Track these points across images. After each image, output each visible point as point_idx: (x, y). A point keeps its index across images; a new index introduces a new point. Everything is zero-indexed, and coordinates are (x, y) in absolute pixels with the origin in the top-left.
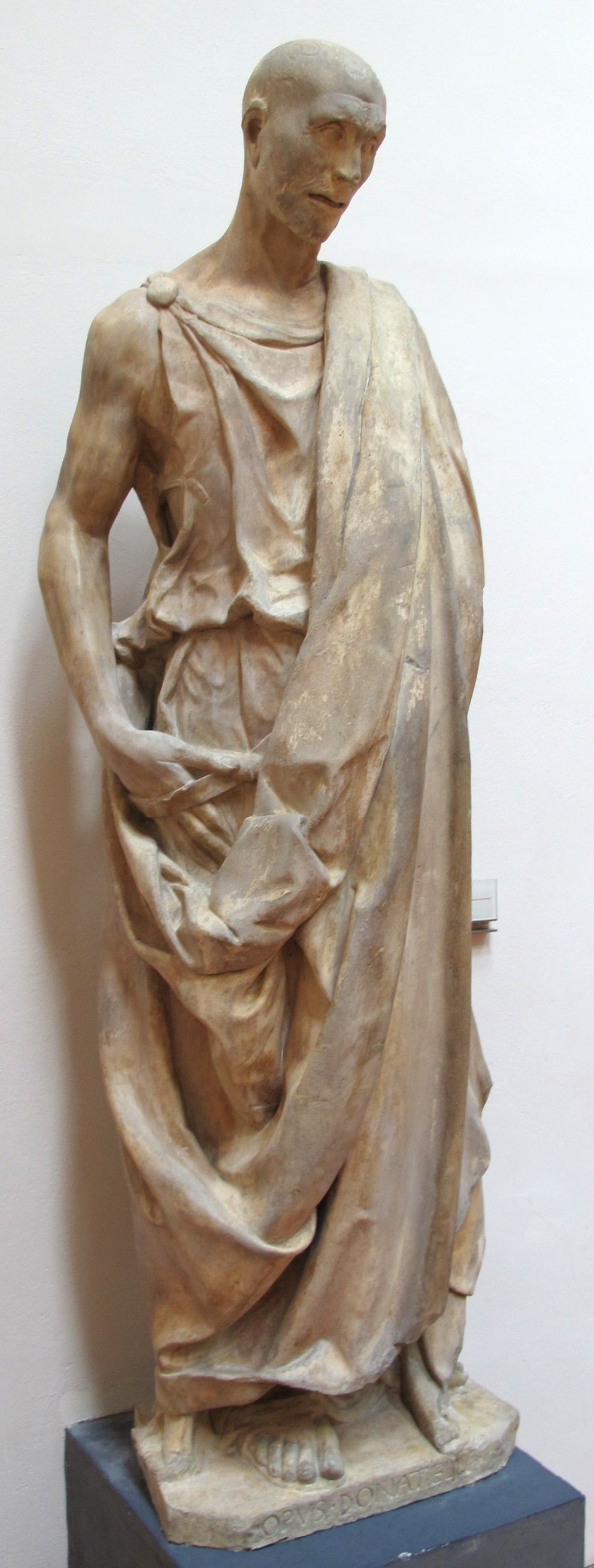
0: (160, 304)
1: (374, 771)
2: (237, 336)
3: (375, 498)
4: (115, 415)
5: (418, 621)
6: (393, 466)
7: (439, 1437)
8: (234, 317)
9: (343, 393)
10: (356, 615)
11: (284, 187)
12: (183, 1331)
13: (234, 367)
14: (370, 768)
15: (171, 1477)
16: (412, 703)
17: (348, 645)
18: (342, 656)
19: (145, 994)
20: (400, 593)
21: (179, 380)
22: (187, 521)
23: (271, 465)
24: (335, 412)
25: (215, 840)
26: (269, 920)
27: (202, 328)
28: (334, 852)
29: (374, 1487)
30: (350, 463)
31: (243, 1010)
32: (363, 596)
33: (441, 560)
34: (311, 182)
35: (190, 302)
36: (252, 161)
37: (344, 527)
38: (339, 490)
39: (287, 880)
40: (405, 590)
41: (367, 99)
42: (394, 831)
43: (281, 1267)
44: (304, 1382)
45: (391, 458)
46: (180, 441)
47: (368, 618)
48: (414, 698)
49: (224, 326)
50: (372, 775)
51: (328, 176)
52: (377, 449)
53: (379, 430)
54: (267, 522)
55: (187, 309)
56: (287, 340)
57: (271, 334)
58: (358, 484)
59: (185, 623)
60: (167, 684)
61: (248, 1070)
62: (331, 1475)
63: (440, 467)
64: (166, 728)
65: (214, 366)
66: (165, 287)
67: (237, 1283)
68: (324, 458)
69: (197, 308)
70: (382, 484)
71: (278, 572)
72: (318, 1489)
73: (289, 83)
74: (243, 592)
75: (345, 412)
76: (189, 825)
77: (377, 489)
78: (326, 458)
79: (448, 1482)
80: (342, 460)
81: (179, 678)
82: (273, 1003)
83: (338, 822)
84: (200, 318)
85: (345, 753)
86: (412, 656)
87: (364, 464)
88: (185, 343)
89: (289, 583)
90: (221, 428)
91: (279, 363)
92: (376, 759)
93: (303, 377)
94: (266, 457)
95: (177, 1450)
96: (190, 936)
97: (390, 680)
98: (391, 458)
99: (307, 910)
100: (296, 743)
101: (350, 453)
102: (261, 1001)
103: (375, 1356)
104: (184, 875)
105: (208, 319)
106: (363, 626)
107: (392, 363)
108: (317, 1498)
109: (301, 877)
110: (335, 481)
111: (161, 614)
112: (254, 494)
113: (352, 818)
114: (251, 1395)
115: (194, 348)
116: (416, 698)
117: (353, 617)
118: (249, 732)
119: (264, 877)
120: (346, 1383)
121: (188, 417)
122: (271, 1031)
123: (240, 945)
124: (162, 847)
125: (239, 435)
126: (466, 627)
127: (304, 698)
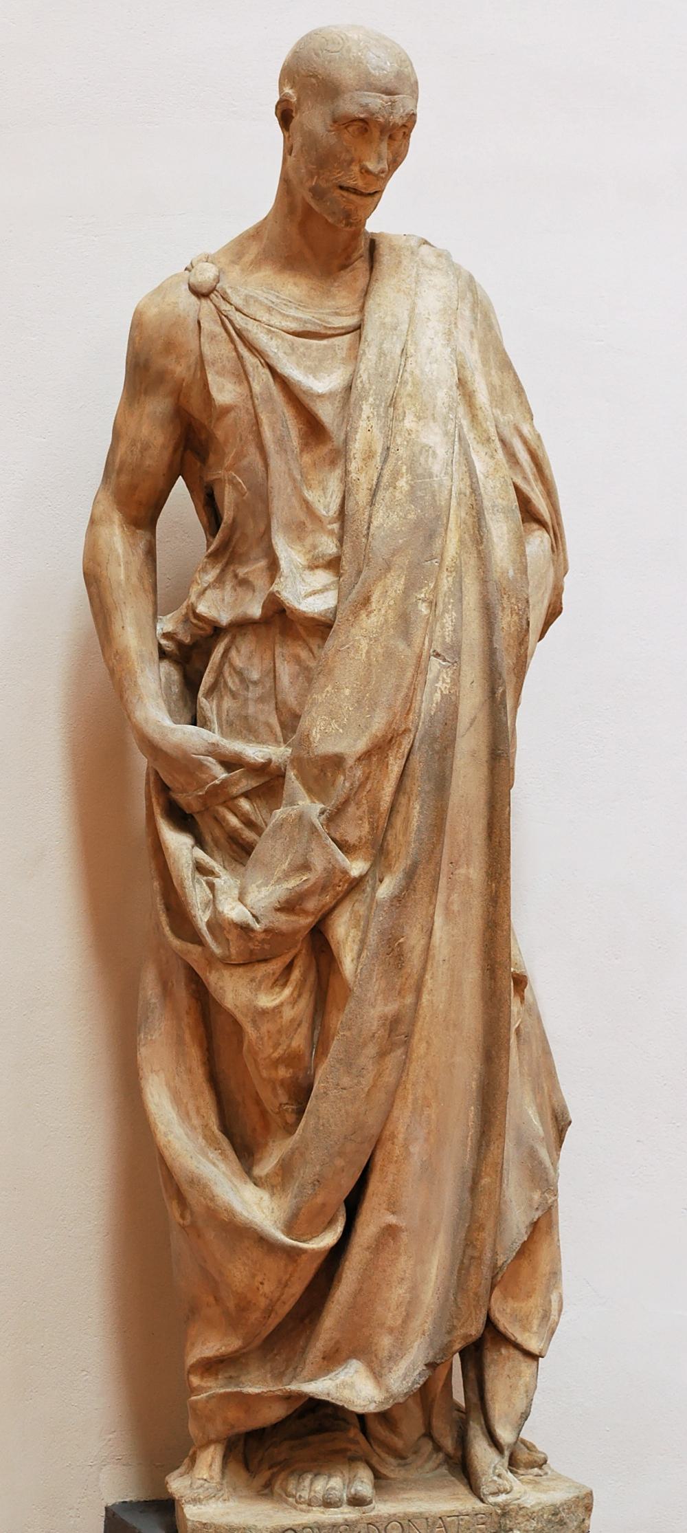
0: (200, 293)
2: (272, 329)
4: (157, 406)
5: (446, 615)
6: (422, 460)
7: (485, 1490)
8: (270, 310)
12: (210, 1346)
13: (271, 362)
14: (391, 760)
15: (196, 1501)
16: (438, 696)
17: (371, 640)
18: (365, 651)
19: (182, 993)
20: (422, 588)
21: (217, 373)
22: (227, 515)
23: (307, 458)
24: (364, 407)
25: (248, 835)
26: (290, 906)
27: (238, 318)
28: (357, 843)
29: (405, 1523)
30: (378, 459)
31: (266, 1001)
33: (479, 552)
35: (229, 291)
36: (288, 150)
37: (370, 523)
38: (365, 486)
39: (305, 867)
40: (427, 585)
41: (389, 93)
42: (414, 823)
43: (307, 1271)
45: (421, 453)
46: (219, 434)
47: (391, 614)
48: (439, 691)
49: (260, 319)
50: (395, 768)
51: (355, 168)
53: (409, 423)
54: (302, 516)
55: (225, 299)
56: (323, 331)
57: (307, 325)
58: (385, 479)
59: (225, 618)
60: (207, 680)
61: (276, 1063)
62: (357, 1501)
64: (205, 724)
65: (250, 359)
66: (207, 274)
68: (352, 454)
69: (237, 300)
70: (410, 478)
71: (312, 567)
72: (342, 1513)
73: (314, 80)
74: (275, 588)
75: (375, 406)
76: (224, 819)
77: (404, 484)
78: (354, 454)
80: (369, 455)
81: (219, 673)
82: (300, 996)
83: (358, 813)
84: (237, 310)
85: (362, 745)
86: (439, 651)
87: (391, 460)
88: (225, 334)
89: (323, 577)
90: (257, 422)
91: (315, 354)
93: (339, 368)
94: (302, 451)
95: (205, 1477)
96: (218, 925)
97: (409, 675)
99: (328, 899)
101: (379, 448)
102: (287, 992)
103: (405, 1376)
104: (217, 867)
105: (245, 311)
106: (386, 621)
107: (430, 350)
108: (341, 1521)
109: (319, 863)
110: (363, 479)
111: (202, 609)
112: (289, 490)
113: (373, 810)
114: (274, 1413)
115: (232, 341)
116: (442, 692)
118: (283, 726)
119: (285, 866)
120: (375, 1402)
121: (226, 410)
122: (299, 1025)
124: (200, 842)
125: (274, 430)
126: (509, 619)
127: (328, 691)
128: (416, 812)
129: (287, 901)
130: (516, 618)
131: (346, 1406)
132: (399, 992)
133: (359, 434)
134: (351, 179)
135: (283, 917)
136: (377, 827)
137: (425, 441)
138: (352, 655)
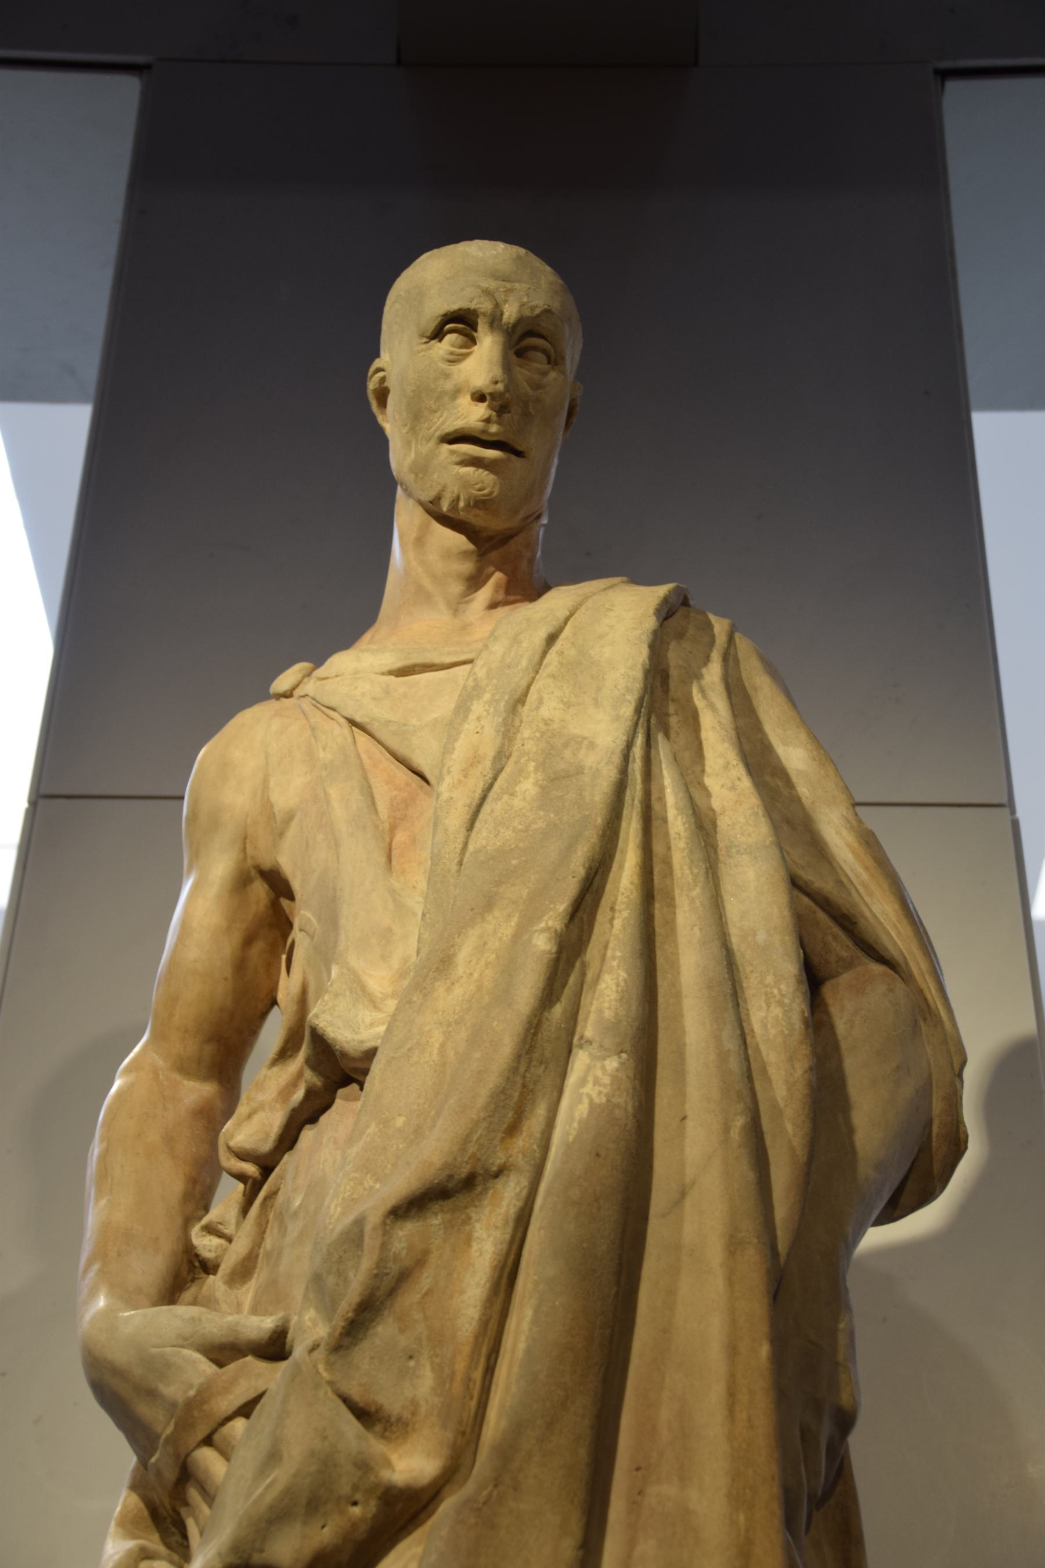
1: (489, 1236)
3: (525, 799)
6: (567, 754)
9: (495, 681)
10: (471, 974)
11: (413, 450)
14: (479, 1230)
16: (583, 1109)
18: (437, 1045)
20: (543, 916)
32: (485, 944)
34: (441, 420)
45: (566, 745)
47: (489, 973)
48: (586, 1101)
52: (538, 735)
63: (722, 786)
70: (540, 778)
78: (449, 768)
83: (404, 1341)
100: (339, 1209)
101: (489, 751)
106: (479, 988)
116: (591, 1100)
126: (762, 1014)
130: (777, 1011)
134: (457, 419)
136: (452, 1375)
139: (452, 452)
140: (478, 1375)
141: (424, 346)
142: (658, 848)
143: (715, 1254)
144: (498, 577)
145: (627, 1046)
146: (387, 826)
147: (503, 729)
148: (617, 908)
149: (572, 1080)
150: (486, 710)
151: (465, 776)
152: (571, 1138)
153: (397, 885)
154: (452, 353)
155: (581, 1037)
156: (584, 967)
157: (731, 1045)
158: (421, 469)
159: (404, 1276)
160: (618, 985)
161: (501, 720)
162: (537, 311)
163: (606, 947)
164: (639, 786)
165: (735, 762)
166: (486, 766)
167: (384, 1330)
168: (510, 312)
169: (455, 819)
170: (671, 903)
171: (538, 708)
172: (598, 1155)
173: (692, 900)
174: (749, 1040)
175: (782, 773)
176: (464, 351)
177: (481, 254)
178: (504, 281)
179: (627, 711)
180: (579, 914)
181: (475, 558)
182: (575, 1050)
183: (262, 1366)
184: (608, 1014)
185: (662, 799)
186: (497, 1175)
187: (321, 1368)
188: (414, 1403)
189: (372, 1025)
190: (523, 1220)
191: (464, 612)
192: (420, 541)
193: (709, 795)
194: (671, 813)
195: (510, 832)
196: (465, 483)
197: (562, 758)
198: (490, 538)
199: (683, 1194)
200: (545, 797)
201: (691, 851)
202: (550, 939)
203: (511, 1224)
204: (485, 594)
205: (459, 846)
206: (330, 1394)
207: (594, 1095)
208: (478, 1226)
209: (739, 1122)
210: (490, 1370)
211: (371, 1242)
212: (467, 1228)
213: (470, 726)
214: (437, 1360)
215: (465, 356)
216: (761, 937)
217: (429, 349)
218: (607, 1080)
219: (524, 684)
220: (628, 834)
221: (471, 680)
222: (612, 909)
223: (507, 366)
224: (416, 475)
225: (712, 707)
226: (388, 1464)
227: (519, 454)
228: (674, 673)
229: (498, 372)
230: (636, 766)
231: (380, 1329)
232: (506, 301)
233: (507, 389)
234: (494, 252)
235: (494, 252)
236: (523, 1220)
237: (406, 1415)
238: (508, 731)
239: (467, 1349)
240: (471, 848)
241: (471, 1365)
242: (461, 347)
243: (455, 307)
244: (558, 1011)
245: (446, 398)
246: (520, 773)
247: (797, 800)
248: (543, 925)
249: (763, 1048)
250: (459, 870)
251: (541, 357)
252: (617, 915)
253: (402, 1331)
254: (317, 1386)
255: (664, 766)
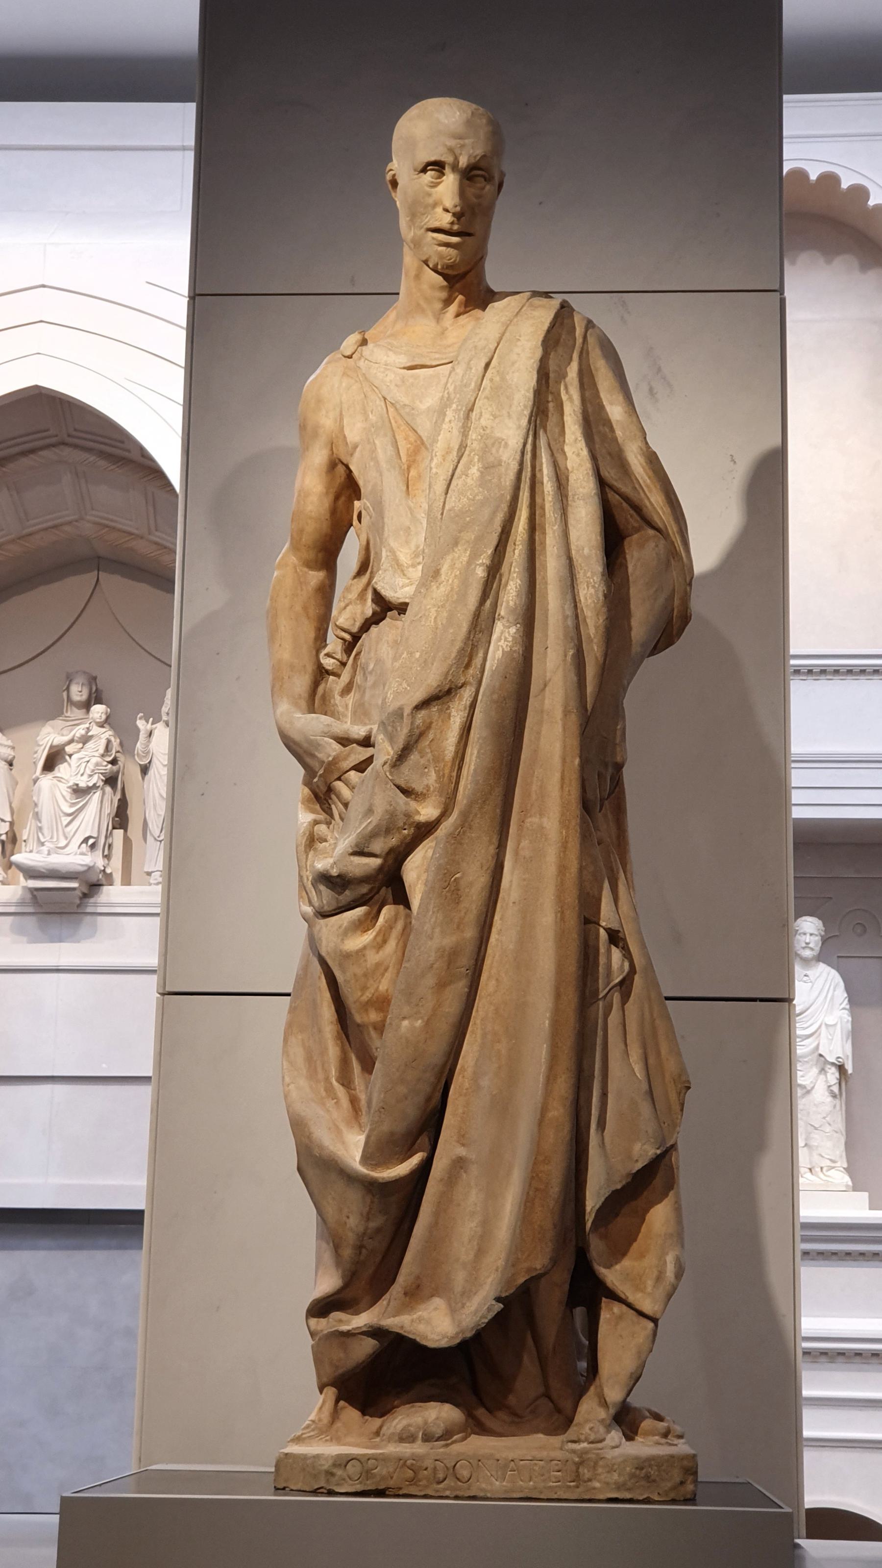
3: (473, 479)
6: (494, 451)
9: (458, 396)
14: (454, 712)
16: (499, 654)
29: (474, 1462)
32: (454, 564)
34: (427, 220)
38: (442, 478)
40: (485, 552)
44: (402, 1327)
45: (493, 444)
48: (501, 649)
50: (457, 719)
52: (479, 437)
63: (574, 453)
67: (348, 1217)
75: (457, 411)
79: (570, 1487)
82: (385, 941)
92: (459, 703)
98: (493, 444)
99: (393, 841)
106: (452, 589)
116: (503, 649)
117: (445, 583)
122: (386, 970)
123: (336, 874)
126: (585, 592)
128: (474, 758)
129: (357, 845)
130: (592, 591)
131: (418, 1339)
132: (458, 927)
133: (441, 435)
135: (357, 860)
136: (444, 775)
137: (498, 435)
138: (423, 623)
139: (433, 238)
140: (454, 774)
141: (416, 176)
142: (538, 500)
143: (558, 714)
144: (460, 297)
145: (520, 621)
146: (406, 466)
147: (462, 430)
148: (517, 543)
149: (494, 637)
150: (454, 417)
151: (444, 460)
152: (494, 668)
153: (412, 505)
154: (432, 182)
155: (499, 615)
156: (501, 575)
157: (569, 612)
158: (417, 244)
159: (422, 734)
160: (516, 588)
161: (461, 424)
162: (478, 158)
163: (511, 566)
164: (529, 469)
165: (580, 439)
166: (454, 455)
167: (414, 757)
168: (463, 162)
169: (439, 487)
170: (544, 533)
171: (480, 419)
172: (506, 677)
173: (554, 532)
174: (578, 605)
175: (608, 423)
176: (438, 180)
177: (446, 122)
178: (459, 139)
179: (524, 422)
180: (499, 548)
181: (447, 290)
182: (496, 621)
183: (360, 749)
184: (511, 603)
185: (541, 470)
186: (461, 687)
187: (388, 774)
188: (427, 786)
189: (403, 587)
190: (473, 706)
191: (442, 319)
192: (418, 277)
193: (566, 459)
194: (546, 479)
195: (466, 499)
196: (441, 257)
197: (492, 454)
198: (455, 276)
199: (545, 686)
200: (483, 482)
201: (554, 503)
202: (484, 570)
203: (468, 709)
204: (453, 308)
205: (442, 504)
206: (393, 786)
207: (504, 647)
208: (453, 710)
209: (571, 652)
210: (460, 768)
211: (406, 720)
212: (448, 711)
213: (445, 426)
214: (437, 769)
215: (439, 183)
216: (586, 551)
217: (420, 178)
218: (510, 639)
219: (473, 399)
220: (523, 500)
221: (446, 392)
222: (515, 544)
223: (462, 193)
224: (415, 245)
225: (570, 399)
226: (418, 813)
227: (469, 235)
228: (552, 375)
229: (457, 200)
230: (528, 457)
231: (412, 757)
232: (461, 154)
233: (462, 209)
234: (453, 120)
235: (453, 120)
236: (473, 706)
237: (425, 791)
238: (465, 432)
239: (450, 764)
240: (447, 507)
241: (452, 770)
242: (437, 179)
243: (433, 159)
244: (488, 603)
245: (430, 208)
246: (471, 462)
247: (615, 439)
248: (481, 561)
249: (585, 610)
250: (442, 518)
251: (483, 180)
252: (517, 547)
253: (421, 757)
254: (387, 783)
255: (543, 450)
